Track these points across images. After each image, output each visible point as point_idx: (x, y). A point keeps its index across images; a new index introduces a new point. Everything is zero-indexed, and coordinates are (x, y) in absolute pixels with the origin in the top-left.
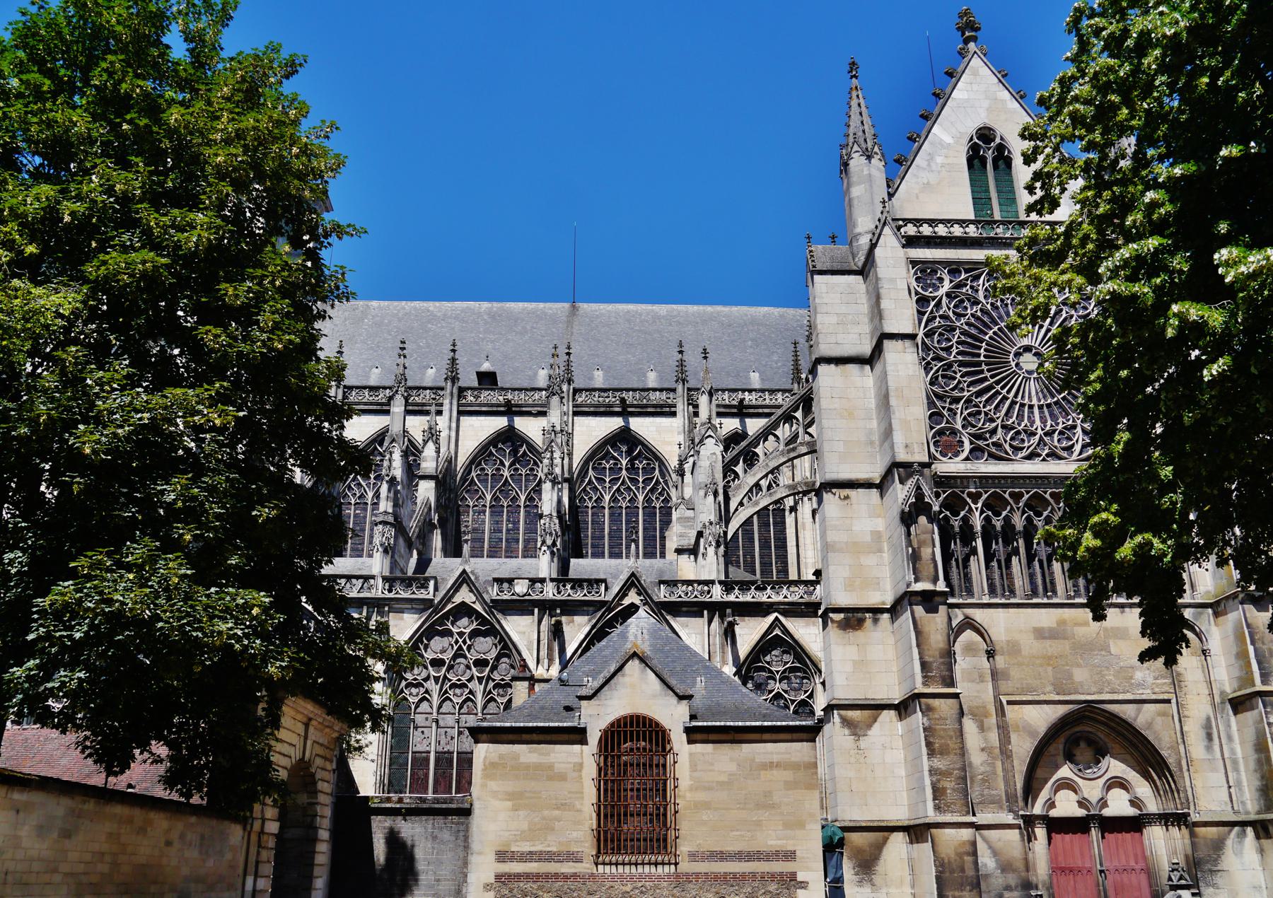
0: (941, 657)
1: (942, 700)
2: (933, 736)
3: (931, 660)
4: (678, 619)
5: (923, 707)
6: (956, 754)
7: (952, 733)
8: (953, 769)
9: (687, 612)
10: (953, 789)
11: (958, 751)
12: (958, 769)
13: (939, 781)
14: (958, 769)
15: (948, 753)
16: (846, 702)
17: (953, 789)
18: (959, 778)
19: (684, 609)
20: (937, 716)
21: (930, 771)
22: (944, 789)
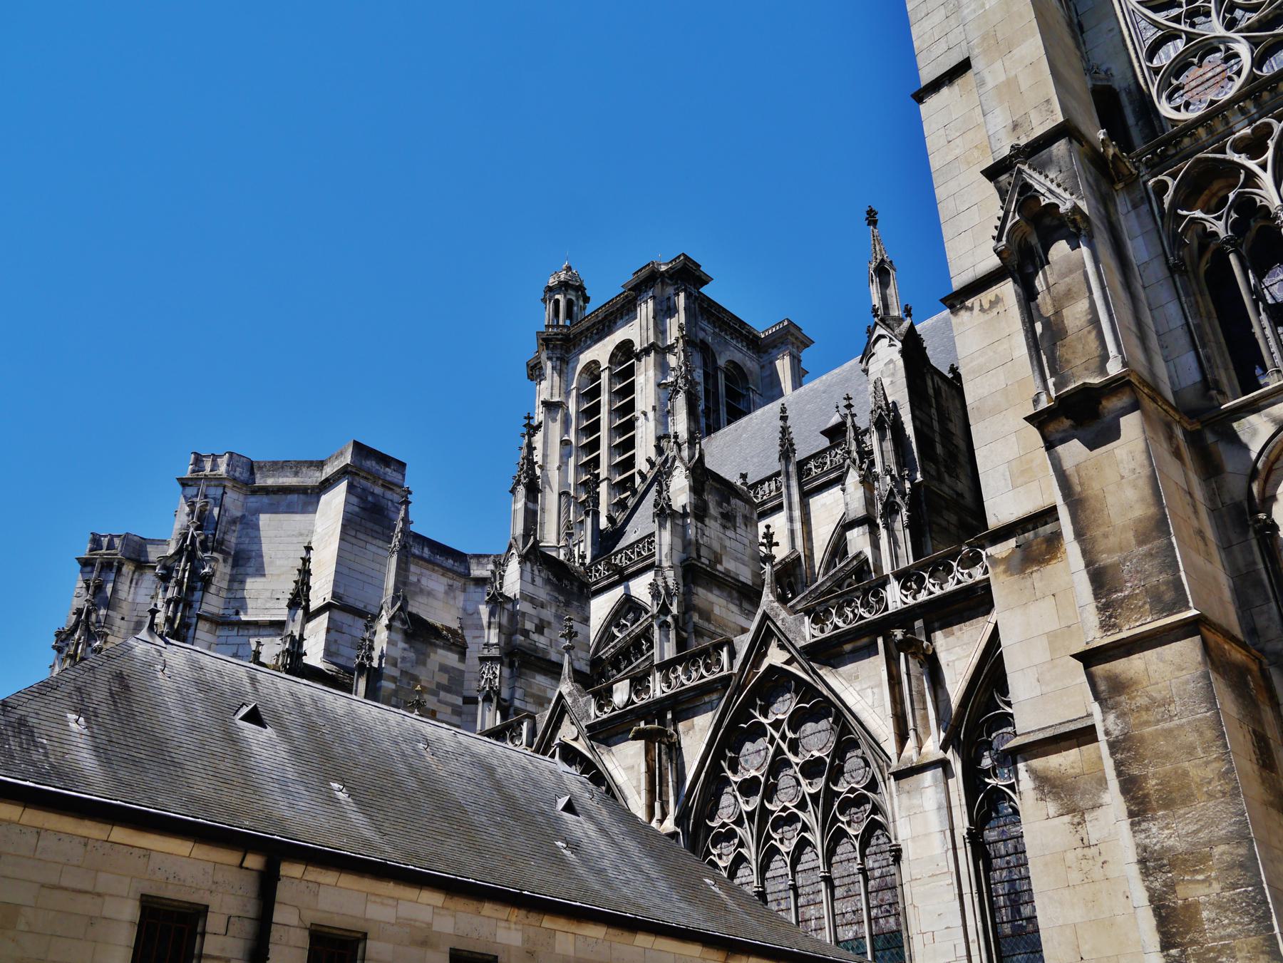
0: (1141, 543)
1: (1150, 654)
2: (1139, 758)
3: (1115, 558)
4: (841, 670)
5: (1102, 687)
6: (1211, 796)
7: (1192, 737)
8: (1211, 844)
9: (853, 651)
10: (1219, 906)
11: (1217, 786)
12: (1227, 840)
13: (1171, 886)
14: (1227, 840)
15: (1188, 799)
16: (1040, 736)
17: (1219, 906)
18: (1231, 867)
19: (848, 647)
20: (1142, 701)
21: (1142, 862)
22: (1191, 909)
